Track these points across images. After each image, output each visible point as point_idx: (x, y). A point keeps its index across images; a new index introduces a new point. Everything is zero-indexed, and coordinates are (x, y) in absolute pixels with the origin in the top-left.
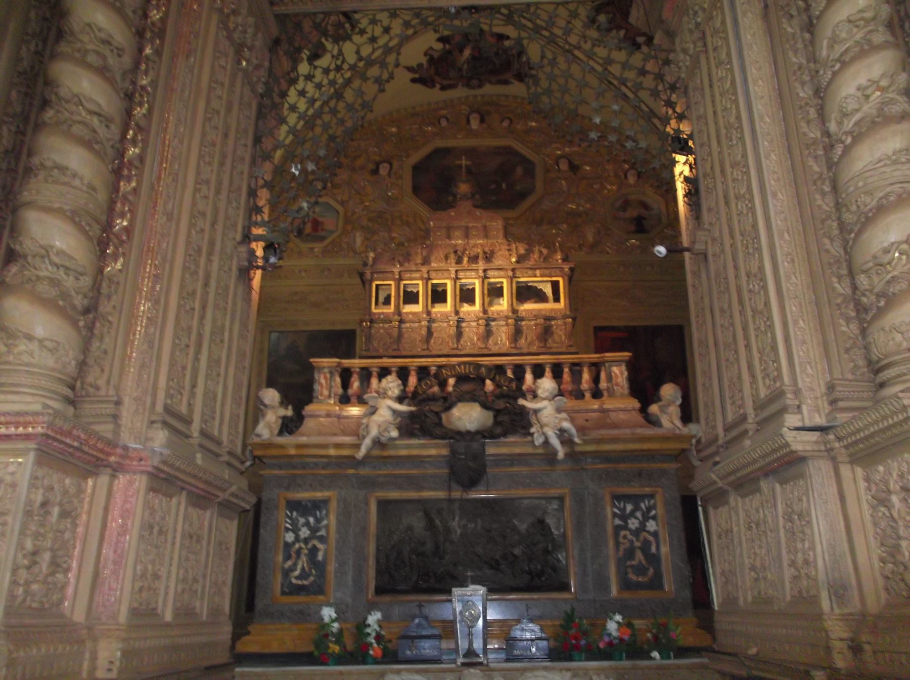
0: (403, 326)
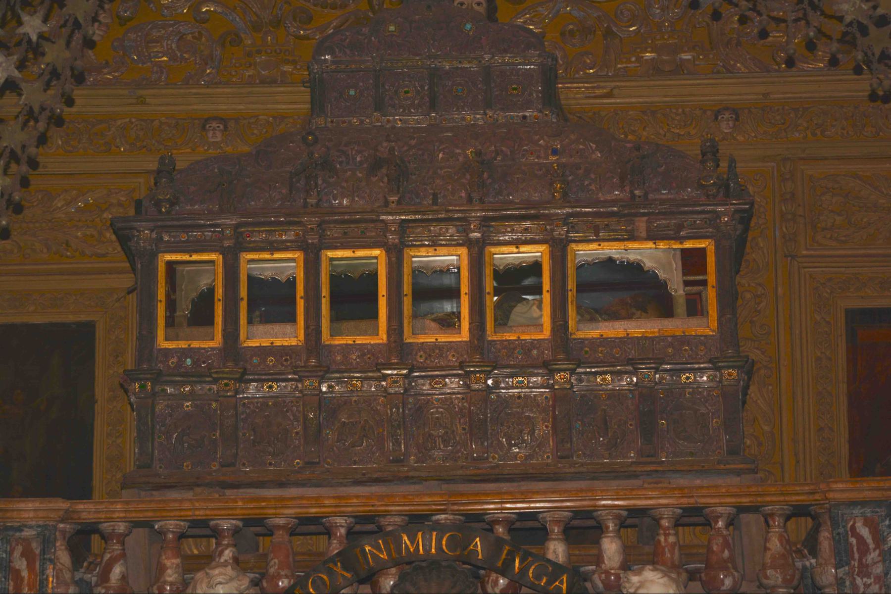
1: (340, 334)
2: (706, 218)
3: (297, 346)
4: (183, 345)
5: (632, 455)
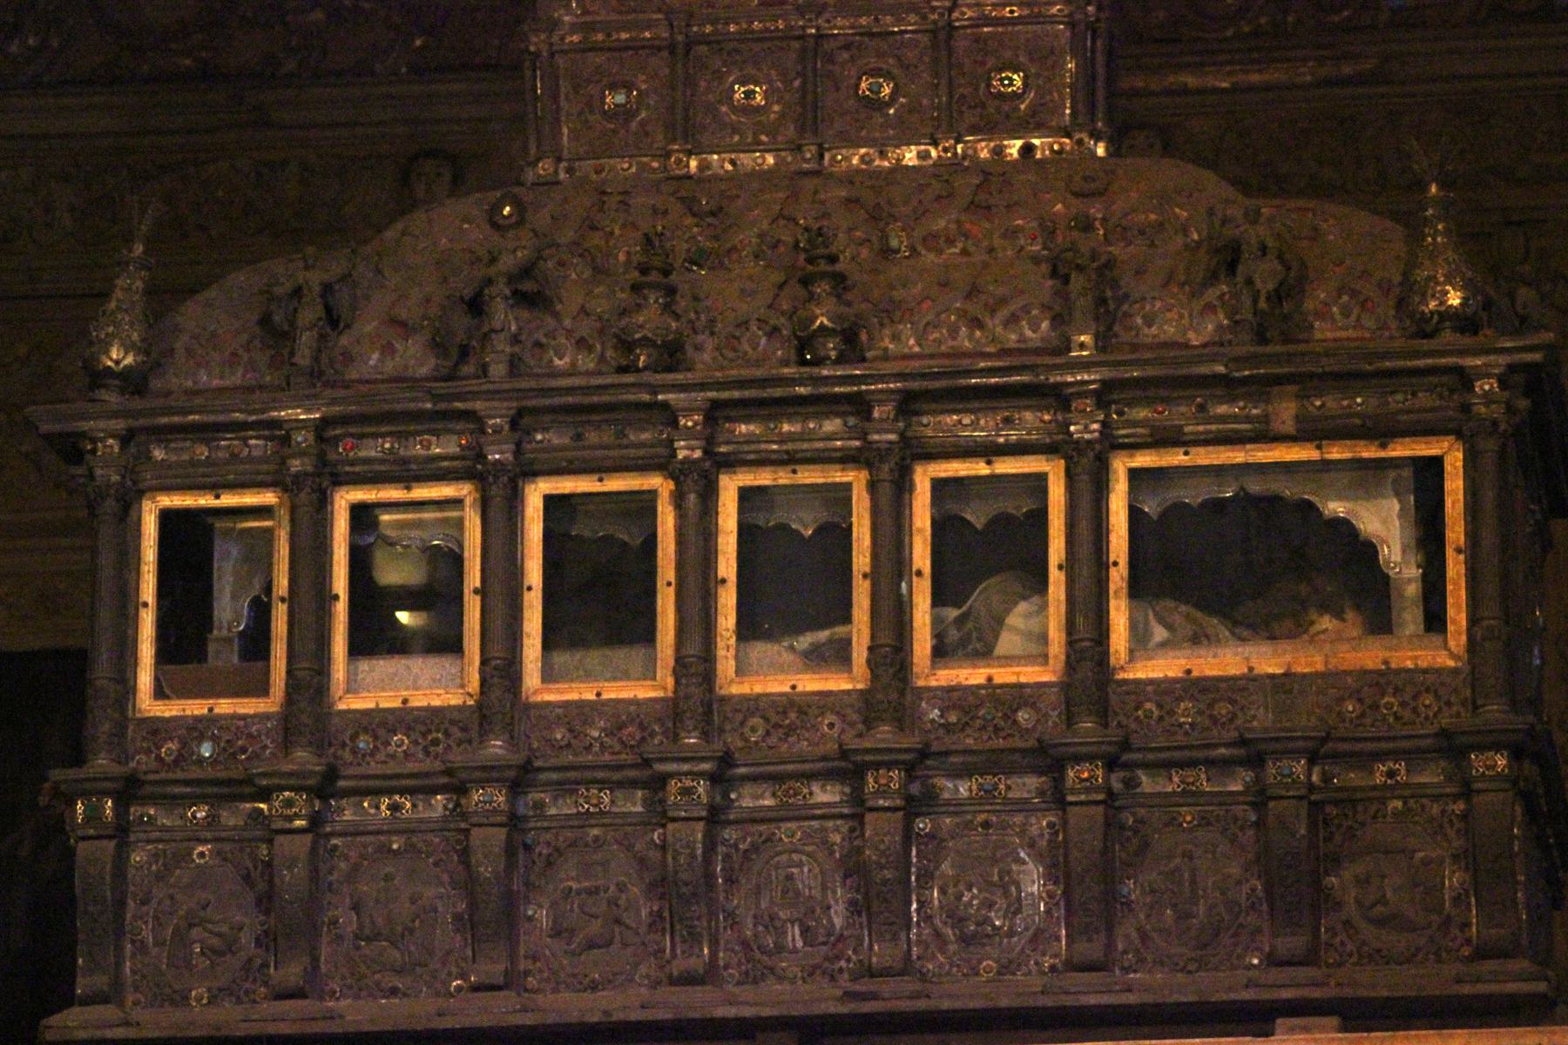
2: (1442, 386)
3: (460, 709)
4: (196, 708)
5: (1256, 961)
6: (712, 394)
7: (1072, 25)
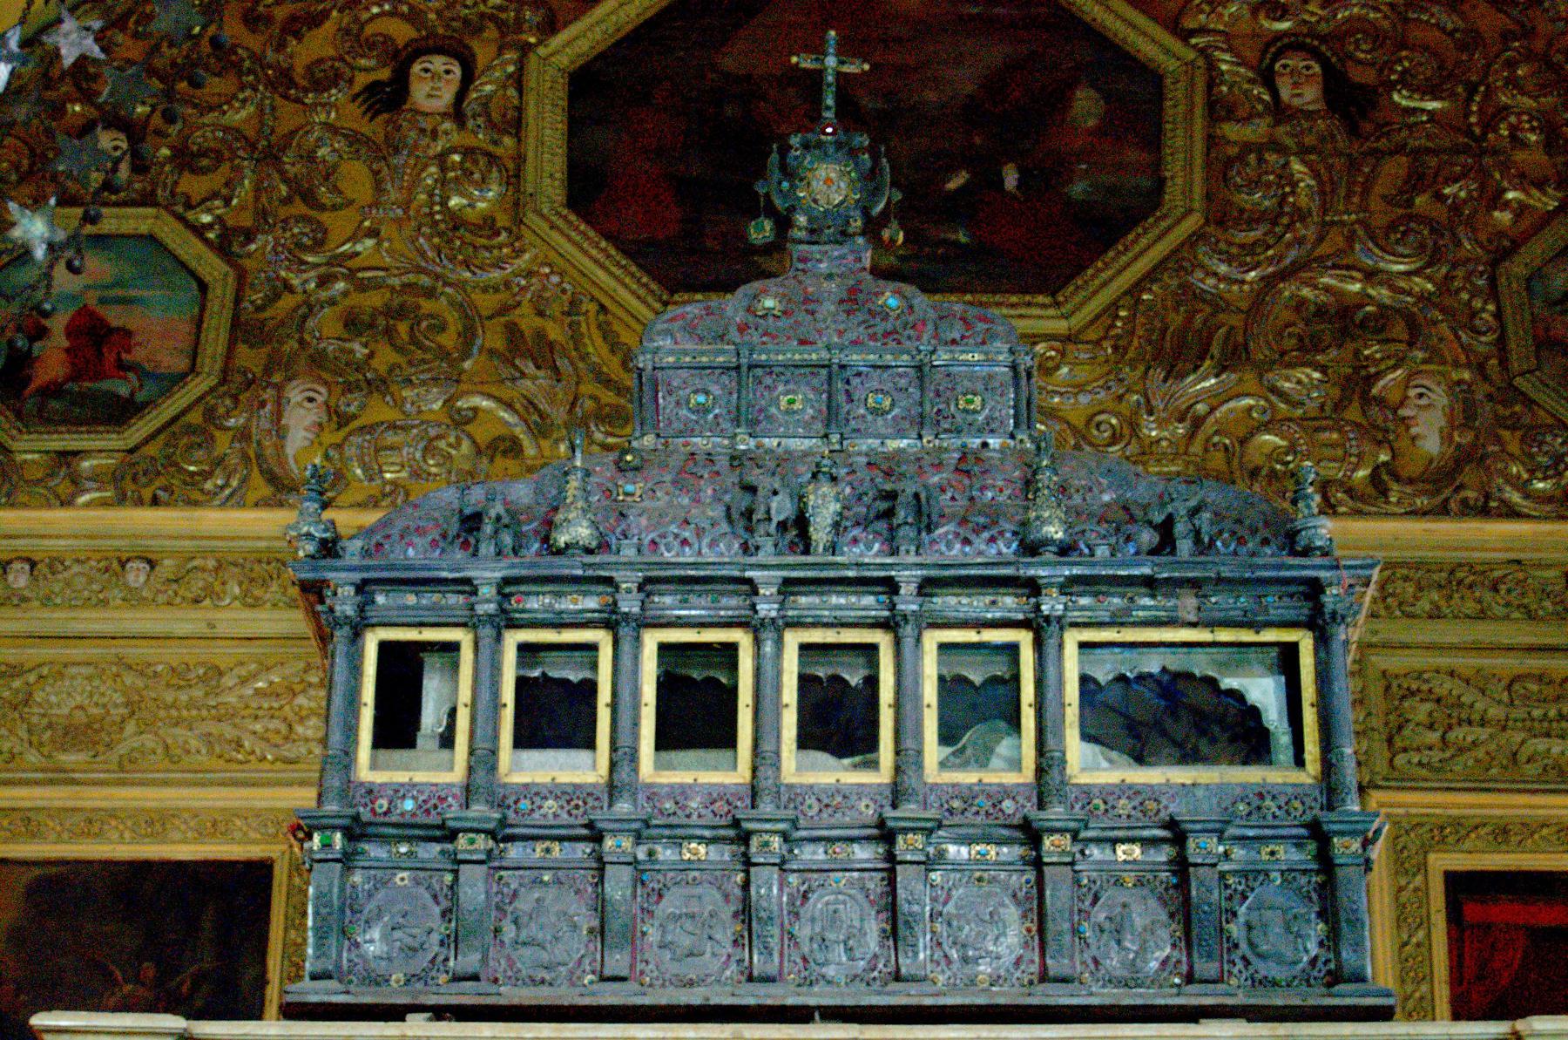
0: (515, 852)
1: (670, 767)
3: (595, 785)
4: (401, 777)
6: (785, 573)
7: (1014, 367)
